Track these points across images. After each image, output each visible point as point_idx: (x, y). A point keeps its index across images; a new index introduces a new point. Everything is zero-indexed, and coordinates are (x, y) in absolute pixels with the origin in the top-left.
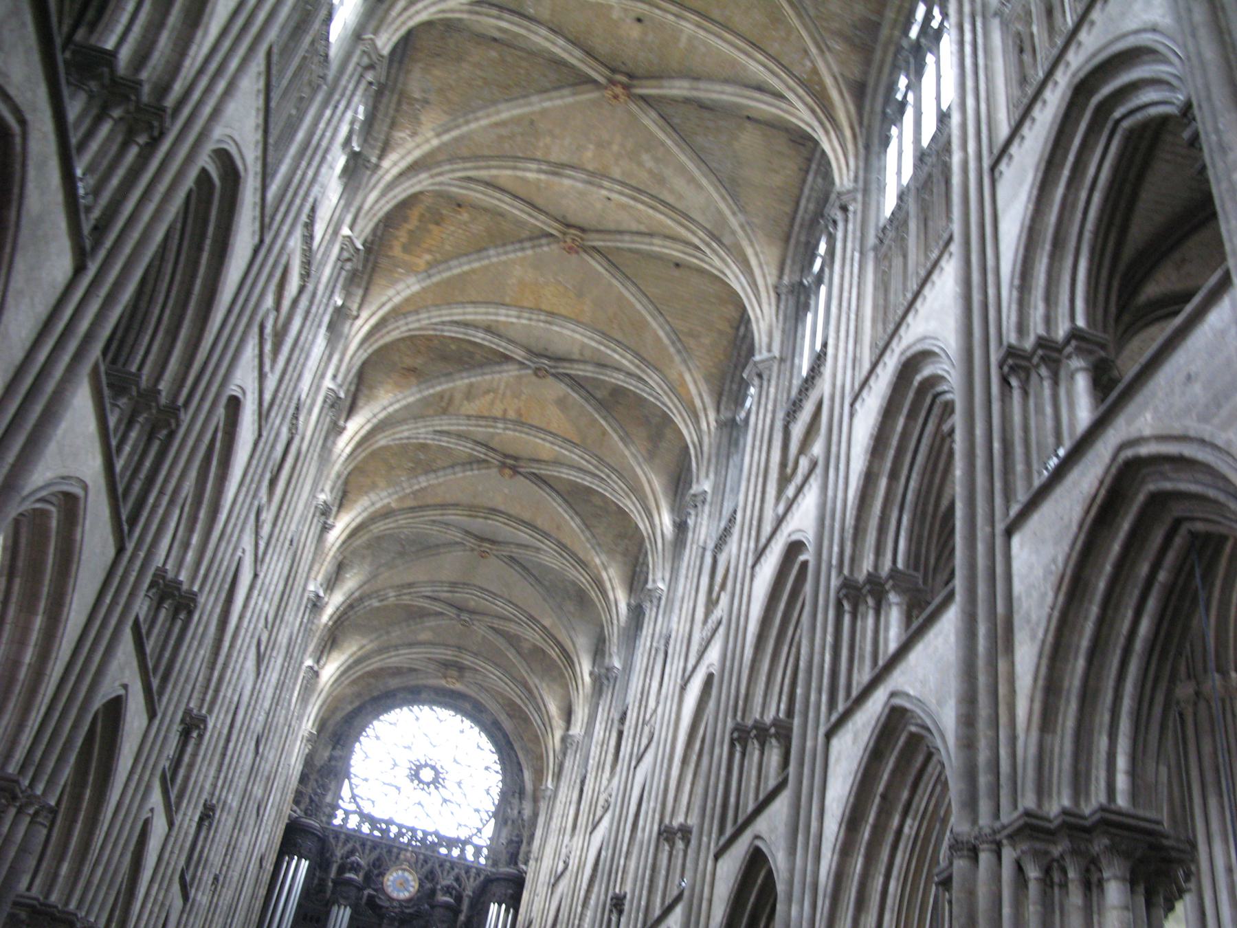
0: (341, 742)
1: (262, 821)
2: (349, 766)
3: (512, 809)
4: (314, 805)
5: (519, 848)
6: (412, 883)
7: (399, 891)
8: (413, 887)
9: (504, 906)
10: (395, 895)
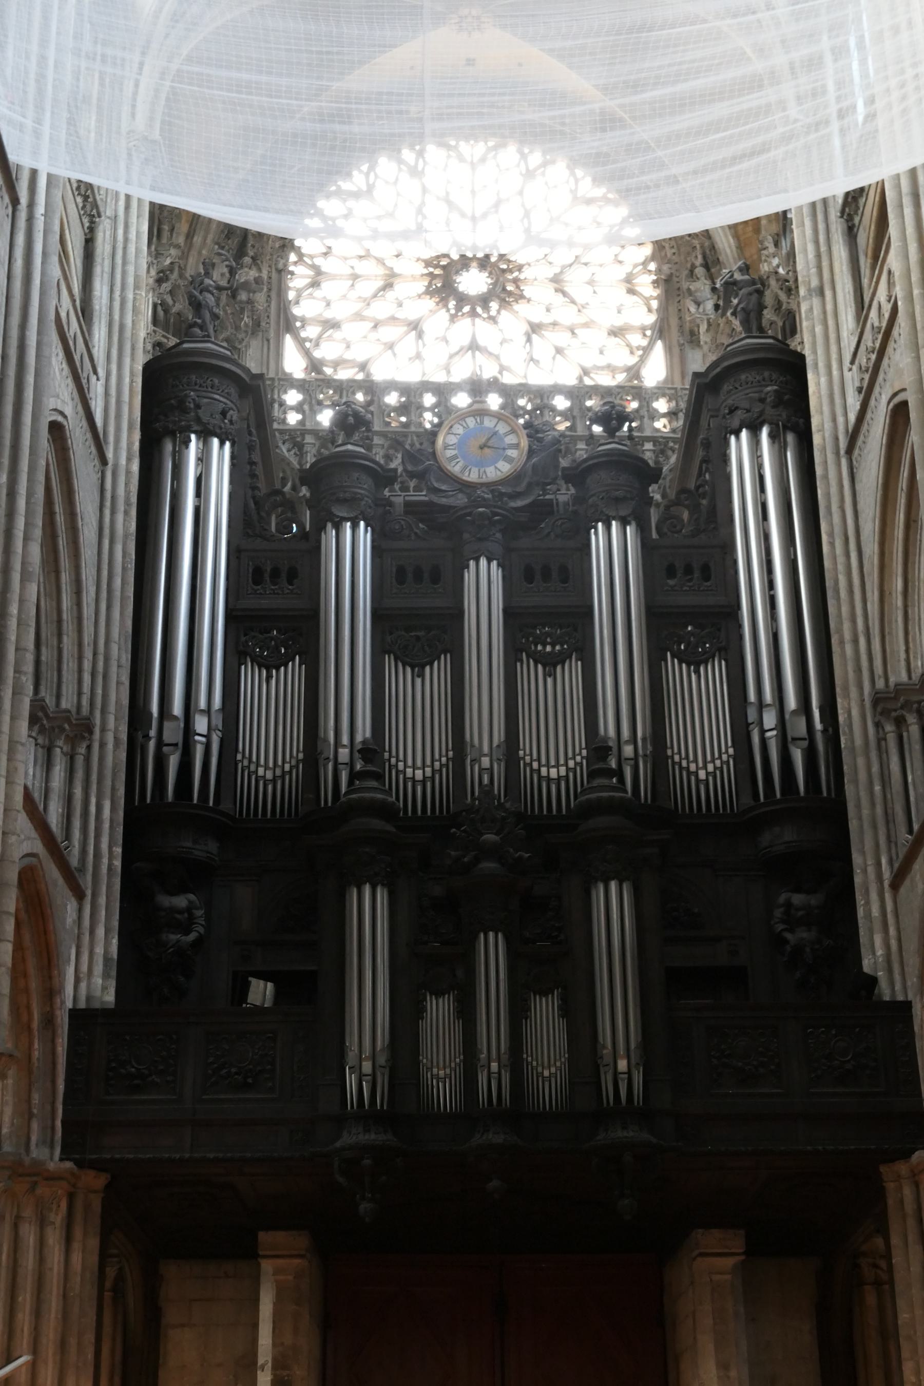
0: (251, 253)
1: (30, 219)
2: (284, 308)
3: (698, 304)
4: (207, 316)
5: (760, 293)
6: (511, 439)
7: (481, 464)
8: (516, 446)
9: (765, 433)
10: (473, 476)
